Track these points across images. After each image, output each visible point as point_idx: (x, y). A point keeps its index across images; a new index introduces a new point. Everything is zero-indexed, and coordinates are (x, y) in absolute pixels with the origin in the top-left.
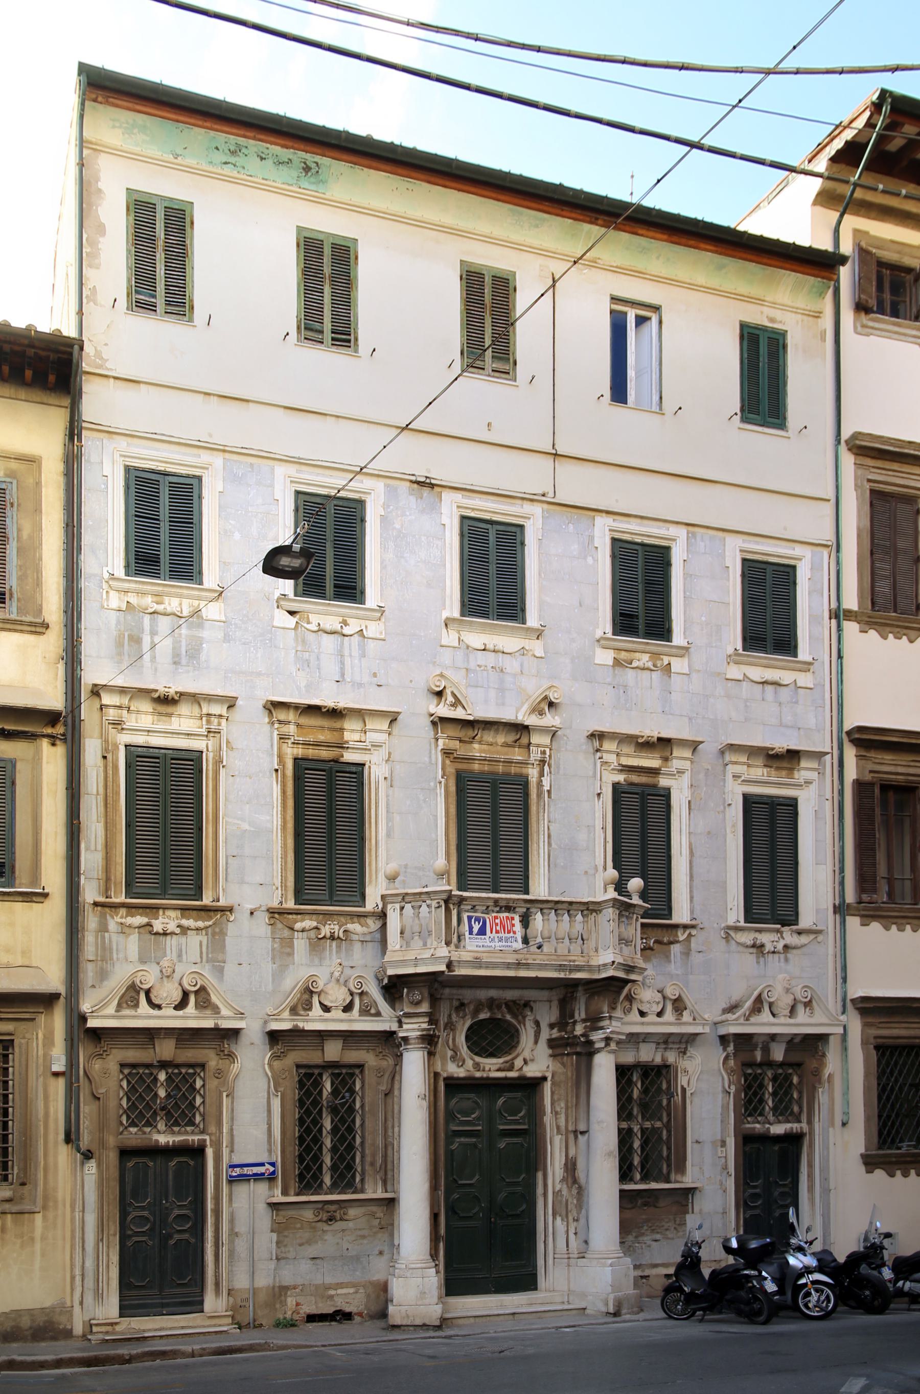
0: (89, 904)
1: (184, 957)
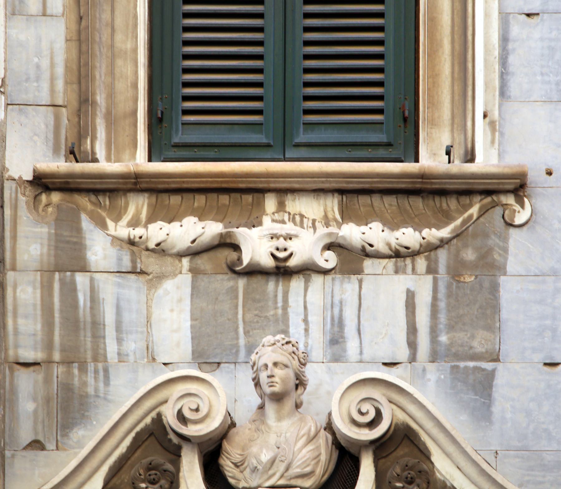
0: (20, 182)
1: (352, 346)
